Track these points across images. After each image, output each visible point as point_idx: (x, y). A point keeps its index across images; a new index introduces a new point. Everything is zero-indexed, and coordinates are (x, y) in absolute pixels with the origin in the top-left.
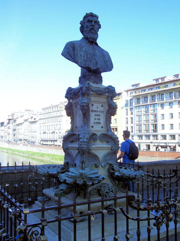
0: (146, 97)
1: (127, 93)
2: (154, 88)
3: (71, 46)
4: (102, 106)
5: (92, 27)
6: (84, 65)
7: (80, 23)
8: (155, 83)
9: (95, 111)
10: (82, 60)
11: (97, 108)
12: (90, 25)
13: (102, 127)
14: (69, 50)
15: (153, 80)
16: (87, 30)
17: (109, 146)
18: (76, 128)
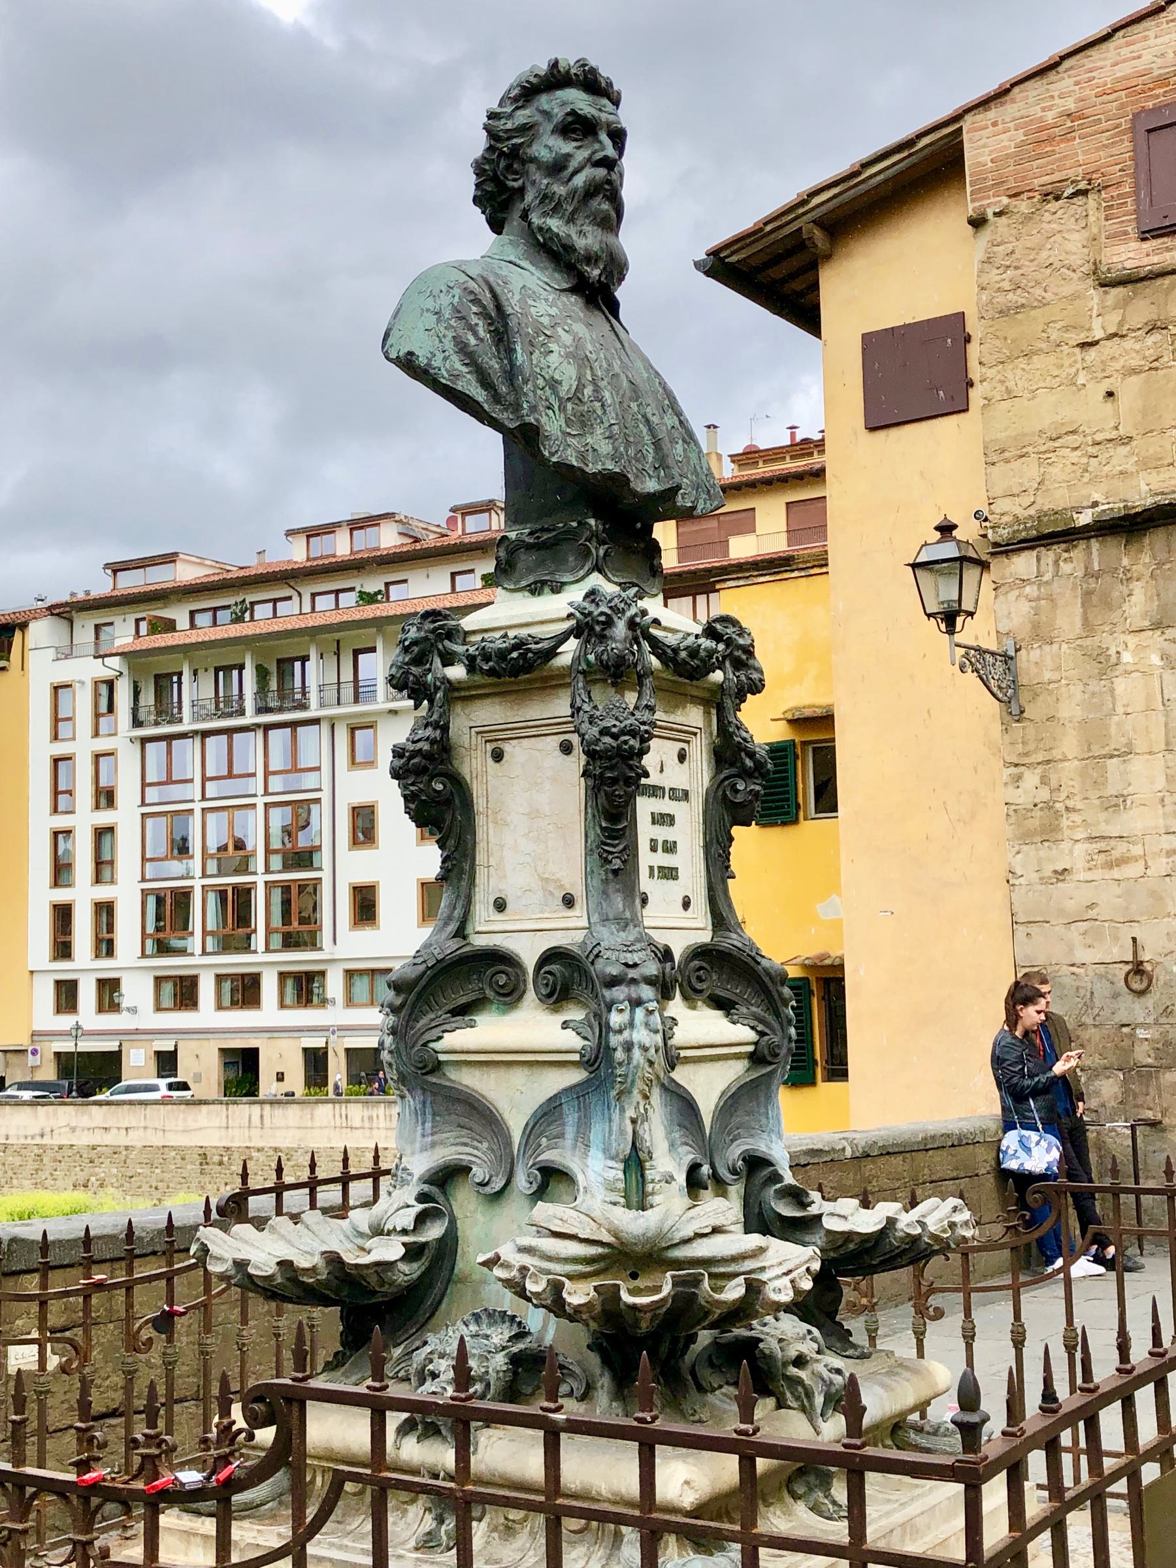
0: (228, 669)
1: (63, 625)
2: (296, 598)
3: (476, 301)
4: (682, 757)
5: (601, 172)
6: (582, 457)
7: (486, 128)
8: (297, 554)
9: (655, 791)
10: (568, 422)
11: (662, 771)
12: (581, 155)
13: (686, 904)
14: (473, 329)
15: (290, 533)
16: (560, 190)
17: (744, 1033)
18: (500, 905)
